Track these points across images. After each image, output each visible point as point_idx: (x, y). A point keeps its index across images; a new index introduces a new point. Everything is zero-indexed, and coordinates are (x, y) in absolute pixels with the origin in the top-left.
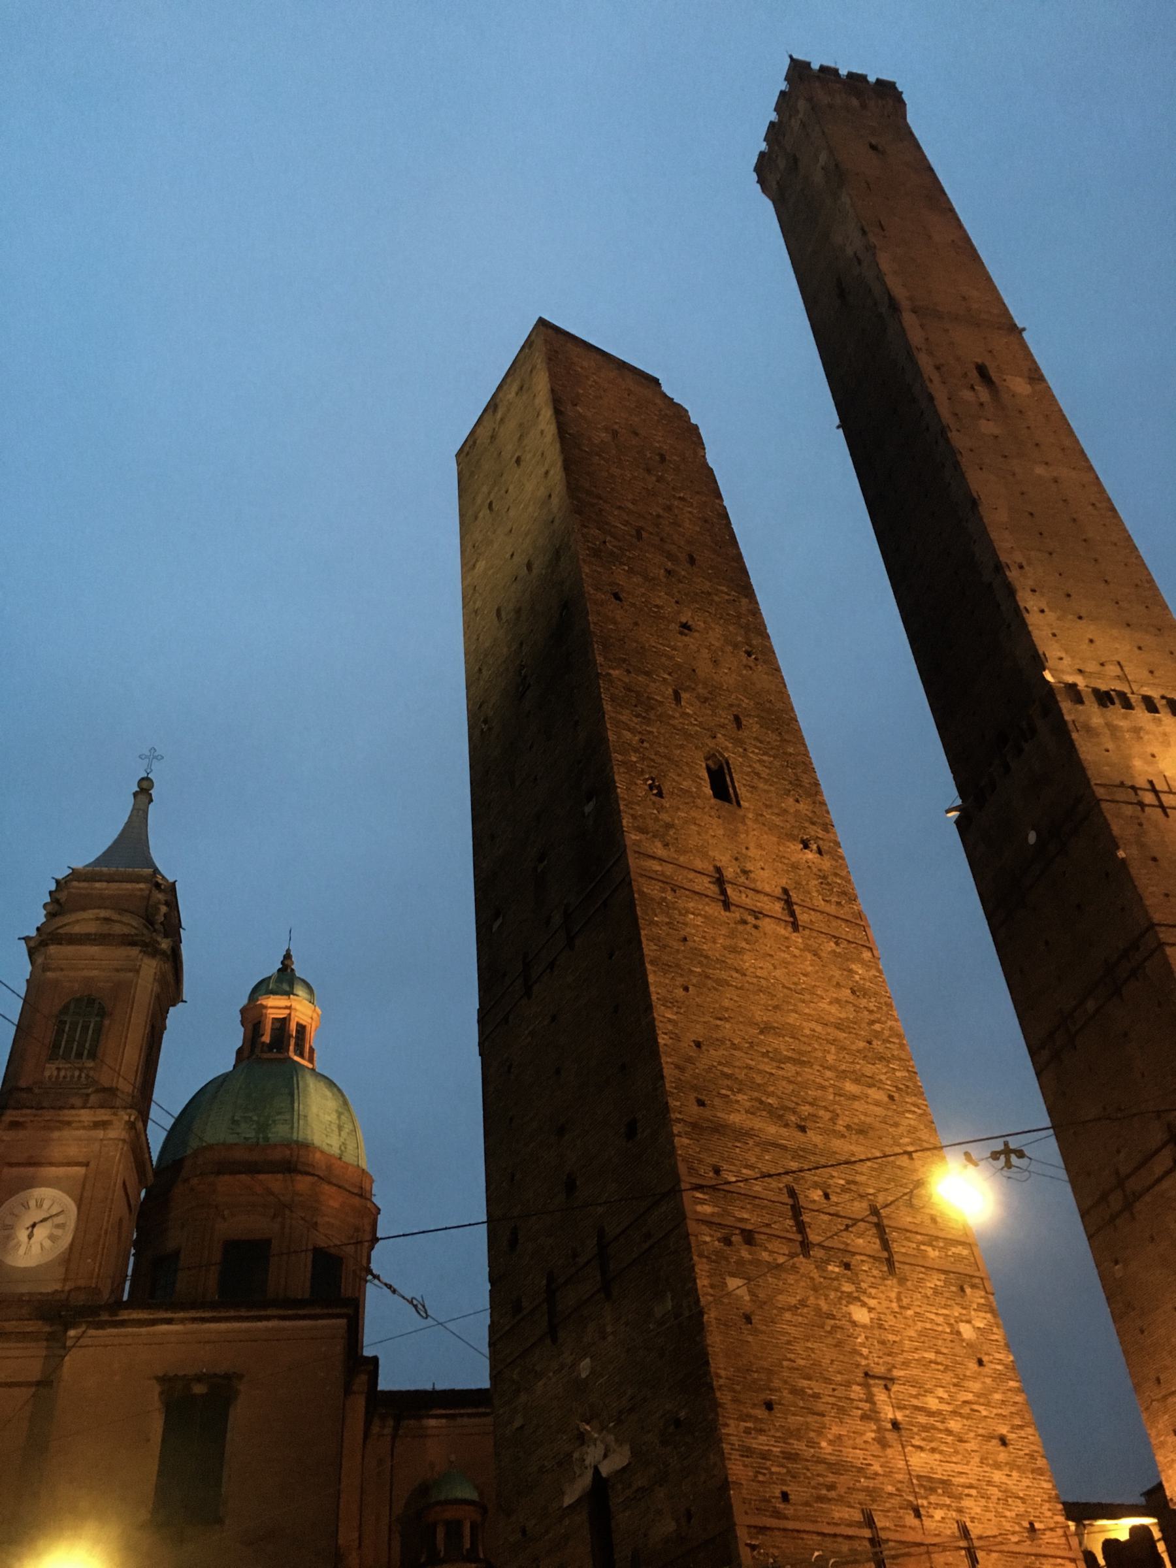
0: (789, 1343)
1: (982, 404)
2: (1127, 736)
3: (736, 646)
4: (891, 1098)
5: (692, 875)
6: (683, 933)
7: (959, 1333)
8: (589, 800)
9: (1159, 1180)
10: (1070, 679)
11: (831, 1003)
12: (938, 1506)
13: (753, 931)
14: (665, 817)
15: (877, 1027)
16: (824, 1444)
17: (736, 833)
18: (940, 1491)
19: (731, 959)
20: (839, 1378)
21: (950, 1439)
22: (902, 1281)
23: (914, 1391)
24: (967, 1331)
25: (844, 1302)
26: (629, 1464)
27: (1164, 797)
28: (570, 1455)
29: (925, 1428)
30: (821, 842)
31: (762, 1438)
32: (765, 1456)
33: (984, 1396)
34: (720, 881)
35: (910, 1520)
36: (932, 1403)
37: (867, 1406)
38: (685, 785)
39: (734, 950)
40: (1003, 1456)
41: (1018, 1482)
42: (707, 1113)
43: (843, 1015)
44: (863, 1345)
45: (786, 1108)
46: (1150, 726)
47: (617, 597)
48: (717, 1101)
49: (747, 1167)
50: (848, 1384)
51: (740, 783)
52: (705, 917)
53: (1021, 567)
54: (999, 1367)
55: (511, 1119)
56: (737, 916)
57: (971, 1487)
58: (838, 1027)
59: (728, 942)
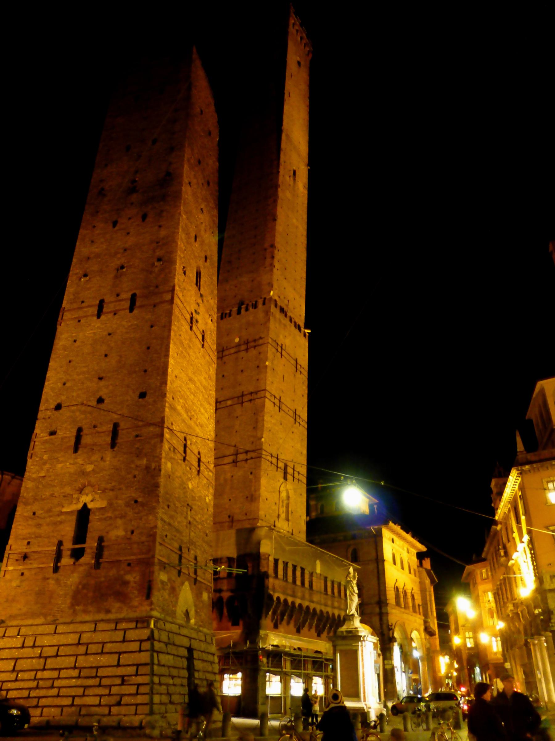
12: (193, 550)
26: (105, 507)
27: (283, 352)
28: (72, 495)
33: (206, 520)
39: (190, 347)
46: (288, 326)
55: (70, 362)
58: (204, 388)
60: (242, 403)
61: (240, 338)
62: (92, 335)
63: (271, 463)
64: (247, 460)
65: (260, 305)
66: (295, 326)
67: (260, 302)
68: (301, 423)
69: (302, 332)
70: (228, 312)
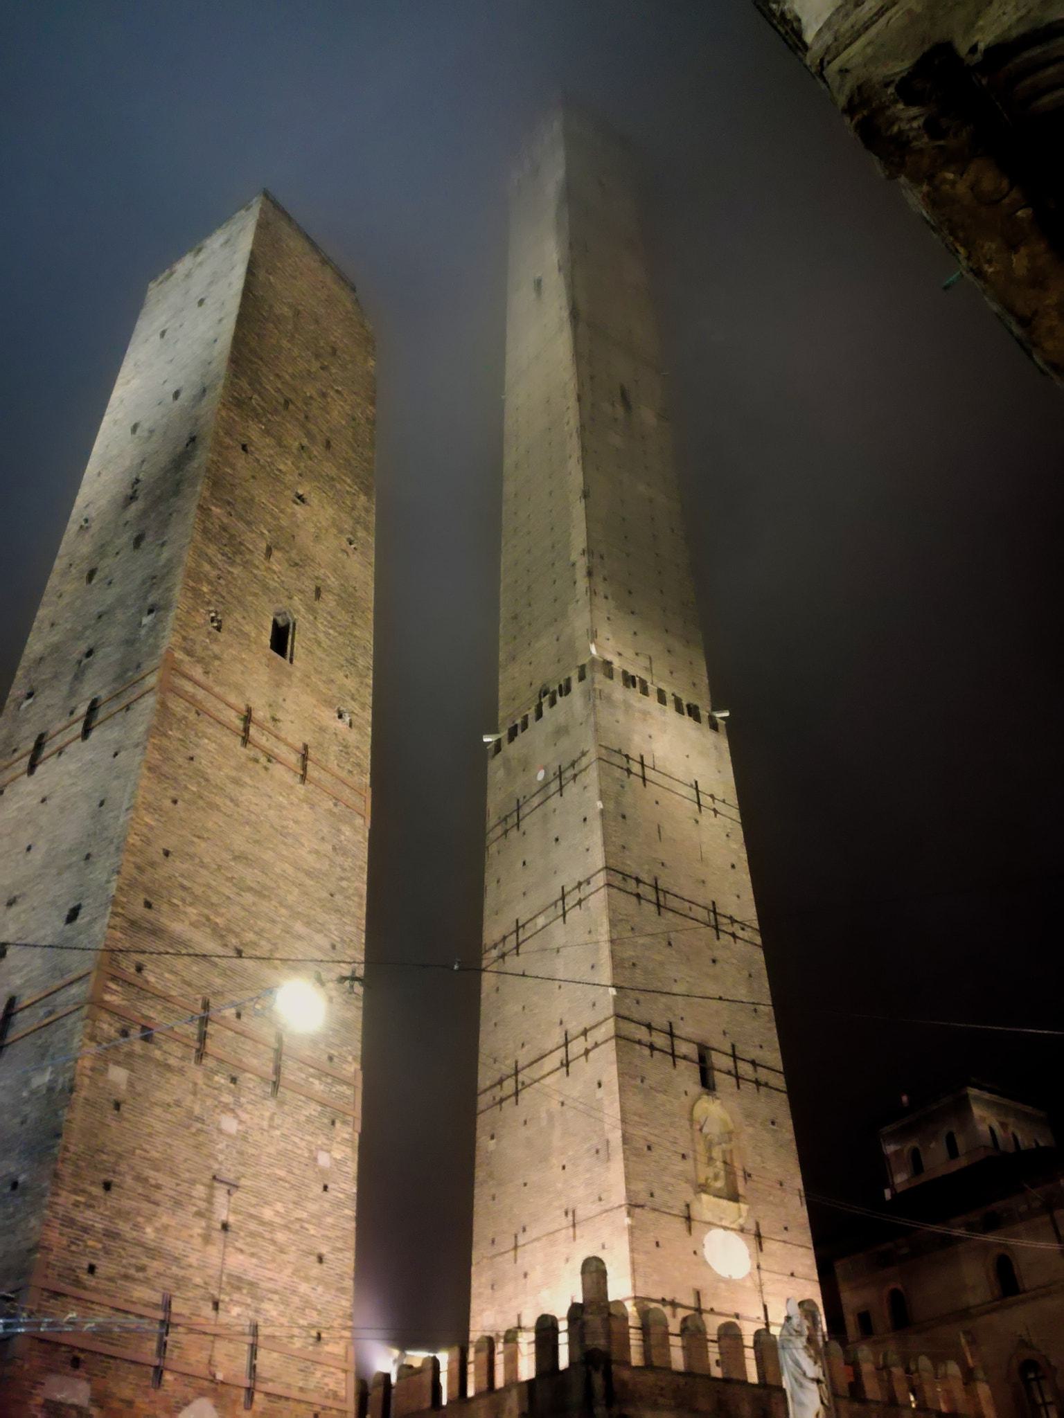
0: (150, 1135)
1: (616, 420)
2: (637, 714)
3: (341, 531)
4: (334, 947)
5: (222, 706)
6: (190, 753)
7: (315, 1159)
8: (150, 611)
9: (543, 1077)
10: (609, 657)
11: (310, 852)
13: (262, 772)
14: (216, 648)
15: (344, 884)
16: (149, 1230)
17: (278, 685)
18: (245, 1291)
19: (230, 788)
20: (187, 1175)
21: (272, 1248)
22: (281, 1103)
23: (254, 1201)
24: (324, 1160)
25: (218, 1111)
29: (252, 1234)
30: (354, 717)
31: (89, 1214)
32: (85, 1230)
33: (317, 1219)
34: (248, 718)
35: (208, 1310)
36: (268, 1214)
37: (203, 1205)
38: (247, 628)
40: (316, 1270)
41: (319, 1295)
42: (150, 915)
43: (318, 866)
44: (221, 1151)
45: (230, 931)
47: (244, 448)
48: (165, 908)
49: (171, 972)
50: (193, 1182)
51: (299, 643)
52: (220, 745)
53: (602, 557)
54: (341, 1196)
56: (252, 754)
57: (275, 1292)
58: (308, 874)
59: (234, 773)
60: (564, 915)
61: (545, 768)
62: (15, 814)
63: (652, 1047)
64: (587, 1052)
65: (575, 685)
66: (679, 709)
67: (574, 675)
68: (740, 933)
69: (705, 719)
70: (519, 721)
